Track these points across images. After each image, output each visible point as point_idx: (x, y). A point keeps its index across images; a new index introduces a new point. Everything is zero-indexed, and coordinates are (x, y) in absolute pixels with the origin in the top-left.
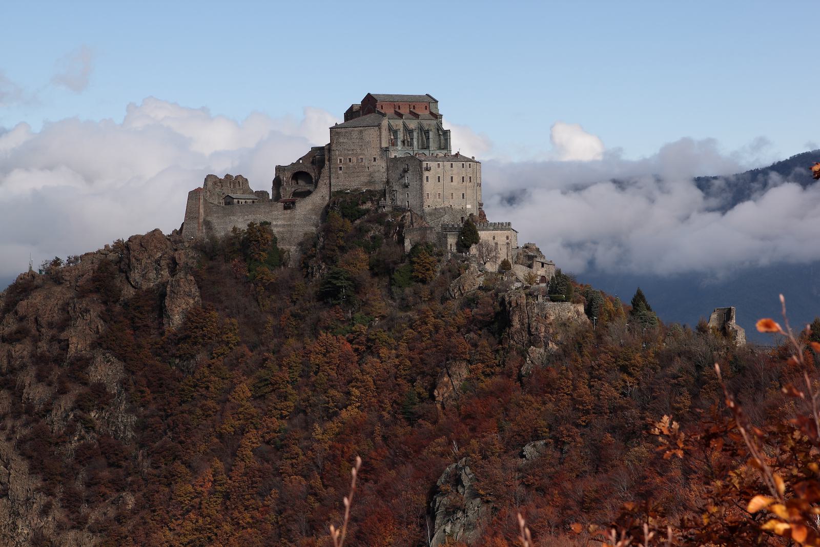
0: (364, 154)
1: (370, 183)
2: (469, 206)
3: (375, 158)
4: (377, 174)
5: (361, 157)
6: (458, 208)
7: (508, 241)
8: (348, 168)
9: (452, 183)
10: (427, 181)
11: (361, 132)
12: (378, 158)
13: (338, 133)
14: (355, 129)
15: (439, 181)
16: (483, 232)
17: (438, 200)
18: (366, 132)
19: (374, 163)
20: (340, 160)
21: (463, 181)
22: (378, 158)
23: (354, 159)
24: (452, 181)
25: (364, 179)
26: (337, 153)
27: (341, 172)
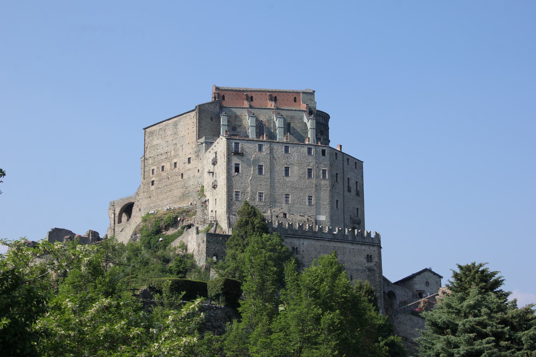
0: (176, 156)
1: (184, 196)
2: (322, 218)
3: (189, 159)
4: (191, 183)
5: (175, 161)
6: (299, 218)
7: (372, 264)
8: (160, 180)
9: (287, 179)
10: (237, 170)
11: (176, 125)
12: (193, 157)
13: (152, 133)
14: (170, 122)
15: (260, 172)
16: (306, 242)
17: (261, 204)
18: (182, 123)
19: (189, 166)
20: (153, 170)
21: (310, 176)
22: (193, 157)
23: (167, 166)
24: (287, 174)
25: (178, 192)
26: (150, 161)
27: (153, 188)
